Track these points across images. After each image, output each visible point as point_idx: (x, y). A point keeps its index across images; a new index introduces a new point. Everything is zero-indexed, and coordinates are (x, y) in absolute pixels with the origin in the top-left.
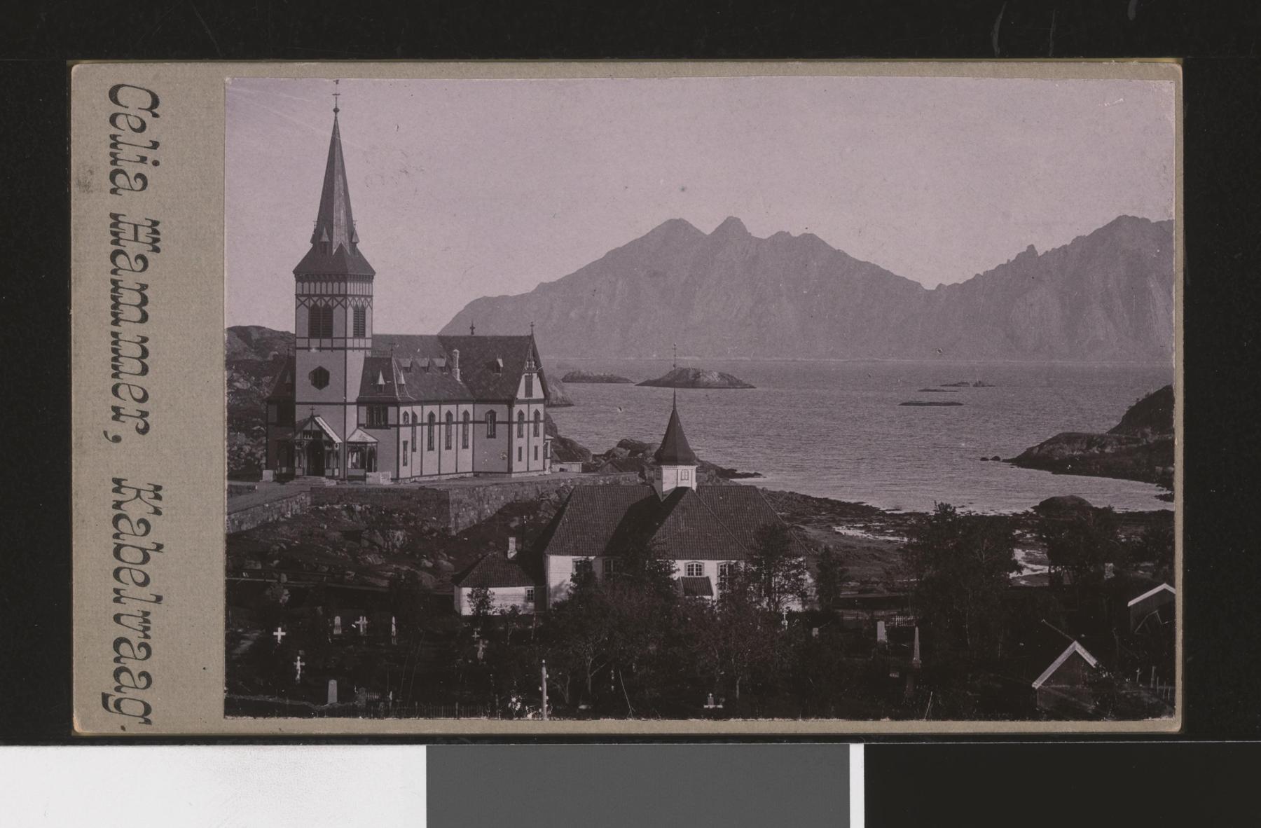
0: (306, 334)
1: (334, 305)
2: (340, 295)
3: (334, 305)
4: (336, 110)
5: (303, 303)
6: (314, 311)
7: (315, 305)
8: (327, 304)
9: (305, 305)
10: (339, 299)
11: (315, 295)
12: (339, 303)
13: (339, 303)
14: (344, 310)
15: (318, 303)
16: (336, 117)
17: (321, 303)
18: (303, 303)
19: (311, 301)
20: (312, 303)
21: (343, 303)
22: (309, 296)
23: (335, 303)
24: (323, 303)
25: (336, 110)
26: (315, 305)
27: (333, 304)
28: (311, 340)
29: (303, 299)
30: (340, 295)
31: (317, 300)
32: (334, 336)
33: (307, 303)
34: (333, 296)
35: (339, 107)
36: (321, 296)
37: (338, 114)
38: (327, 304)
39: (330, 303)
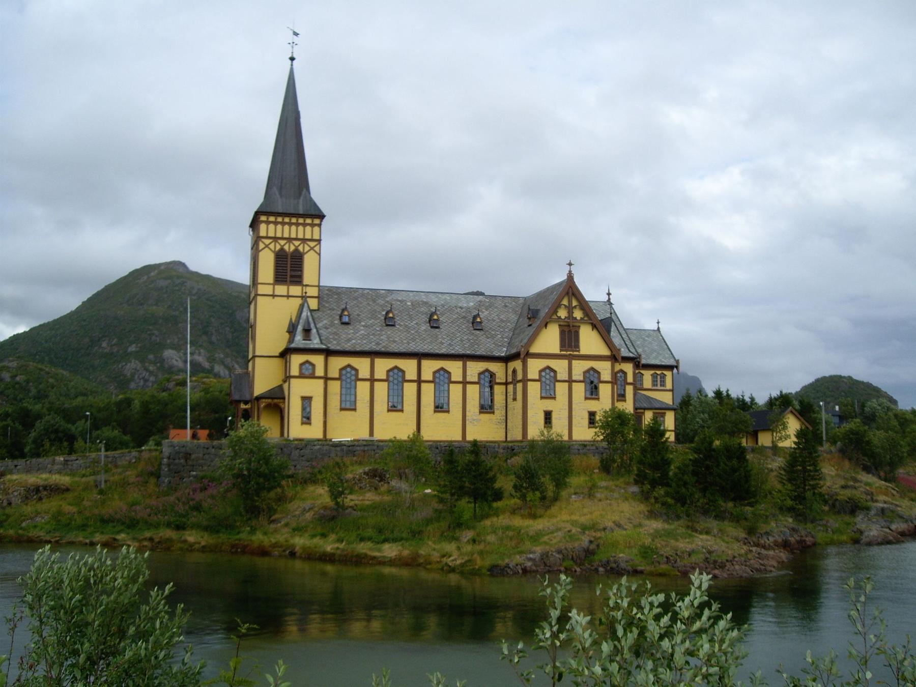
0: (271, 280)
1: (305, 251)
2: (312, 240)
3: (305, 251)
4: (292, 59)
5: (267, 246)
6: (281, 257)
7: (282, 249)
8: (296, 250)
9: (271, 249)
10: (312, 244)
11: (282, 238)
12: (312, 249)
13: (312, 249)
14: (318, 257)
15: (286, 247)
16: (292, 65)
17: (290, 248)
18: (267, 246)
19: (277, 244)
20: (278, 247)
21: (317, 249)
22: (275, 239)
23: (307, 248)
24: (292, 248)
25: (292, 59)
26: (282, 249)
27: (304, 250)
28: (276, 287)
29: (267, 241)
30: (312, 240)
31: (285, 244)
32: (305, 282)
33: (272, 246)
34: (304, 241)
35: (295, 56)
36: (290, 240)
37: (294, 62)
38: (296, 250)
39: (301, 248)
